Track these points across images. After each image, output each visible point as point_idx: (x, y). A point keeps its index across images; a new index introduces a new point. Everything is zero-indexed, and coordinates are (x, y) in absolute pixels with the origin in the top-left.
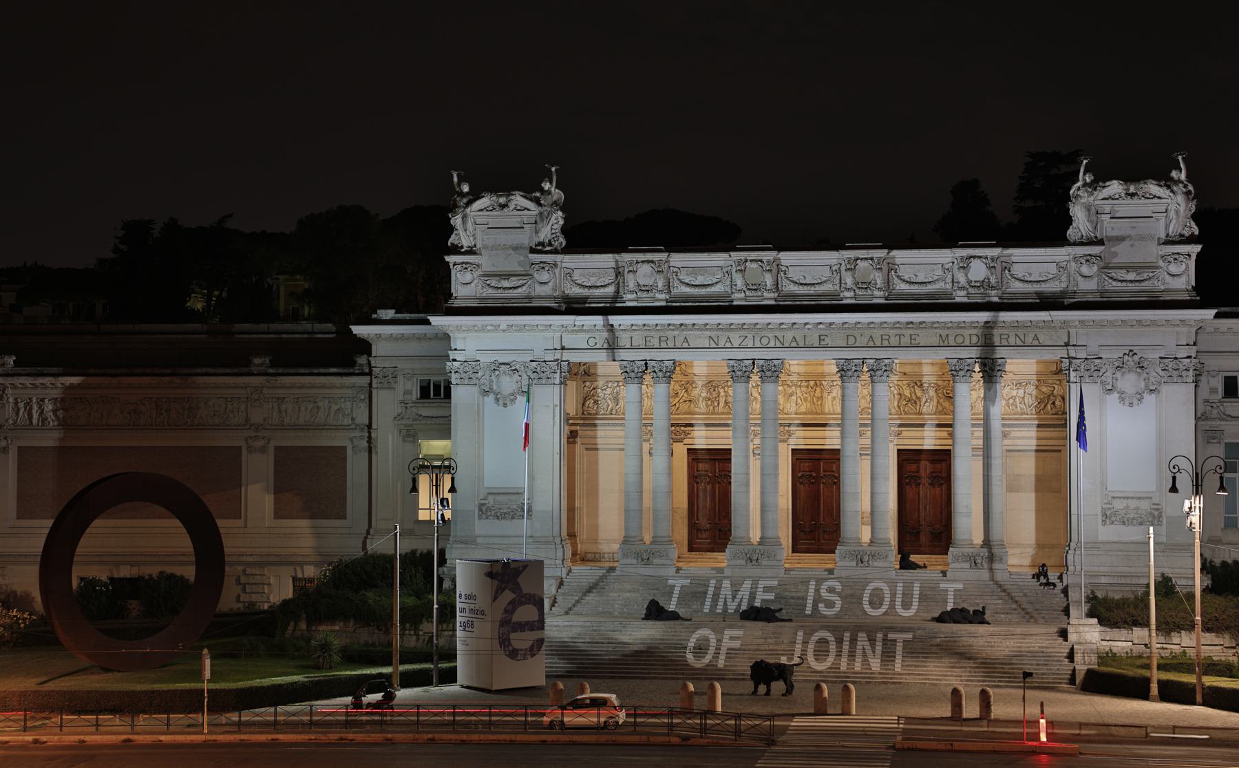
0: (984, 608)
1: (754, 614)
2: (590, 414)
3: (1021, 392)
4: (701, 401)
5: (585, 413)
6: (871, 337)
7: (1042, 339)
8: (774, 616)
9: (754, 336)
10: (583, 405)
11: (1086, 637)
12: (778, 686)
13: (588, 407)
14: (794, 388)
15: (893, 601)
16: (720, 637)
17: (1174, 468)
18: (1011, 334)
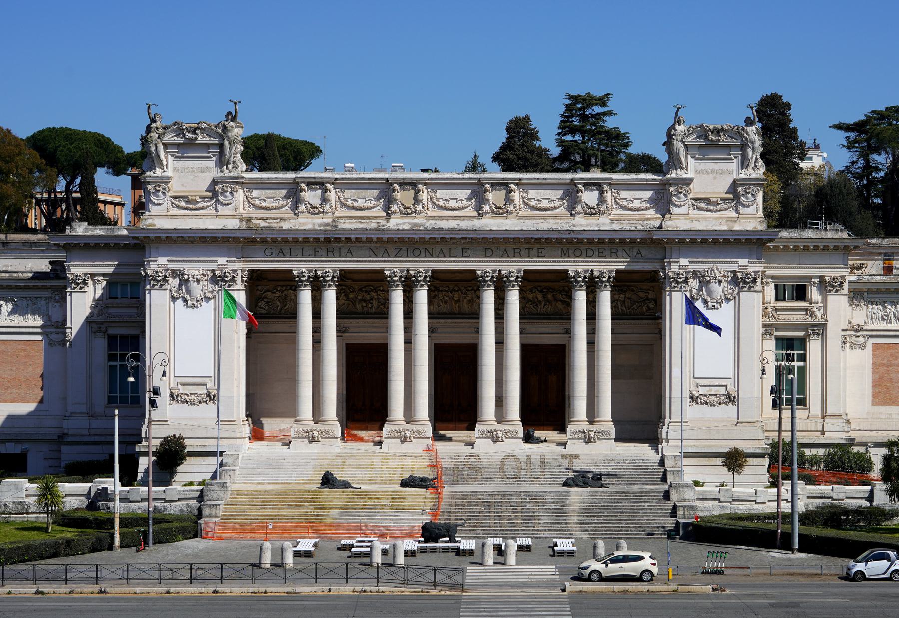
2: (262, 314)
3: (622, 296)
4: (357, 303)
5: (258, 312)
6: (505, 250)
7: (644, 252)
9: (407, 249)
10: (256, 306)
11: (685, 497)
13: (260, 308)
14: (436, 292)
17: (764, 360)
18: (619, 249)
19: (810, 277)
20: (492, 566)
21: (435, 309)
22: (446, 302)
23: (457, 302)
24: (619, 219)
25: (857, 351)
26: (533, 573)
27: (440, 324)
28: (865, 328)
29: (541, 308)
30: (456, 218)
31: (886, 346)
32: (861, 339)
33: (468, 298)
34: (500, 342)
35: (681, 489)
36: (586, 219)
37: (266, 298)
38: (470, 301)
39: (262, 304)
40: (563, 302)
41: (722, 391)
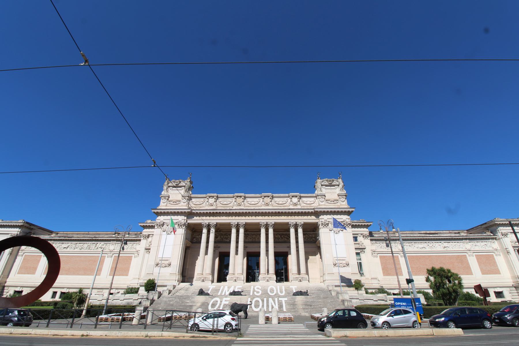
0: (307, 291)
1: (234, 293)
8: (241, 294)
10: (193, 240)
12: (241, 314)
15: (277, 291)
16: (221, 300)
19: (358, 234)
20: (264, 324)
21: (247, 240)
22: (251, 238)
23: (254, 238)
24: (304, 206)
25: (375, 258)
26: (290, 328)
27: (248, 245)
28: (376, 251)
29: (280, 240)
30: (253, 207)
31: (383, 257)
32: (375, 254)
33: (258, 237)
34: (267, 251)
35: (343, 294)
36: (293, 206)
37: (196, 237)
38: (258, 238)
39: (194, 239)
40: (287, 238)
41: (344, 262)
